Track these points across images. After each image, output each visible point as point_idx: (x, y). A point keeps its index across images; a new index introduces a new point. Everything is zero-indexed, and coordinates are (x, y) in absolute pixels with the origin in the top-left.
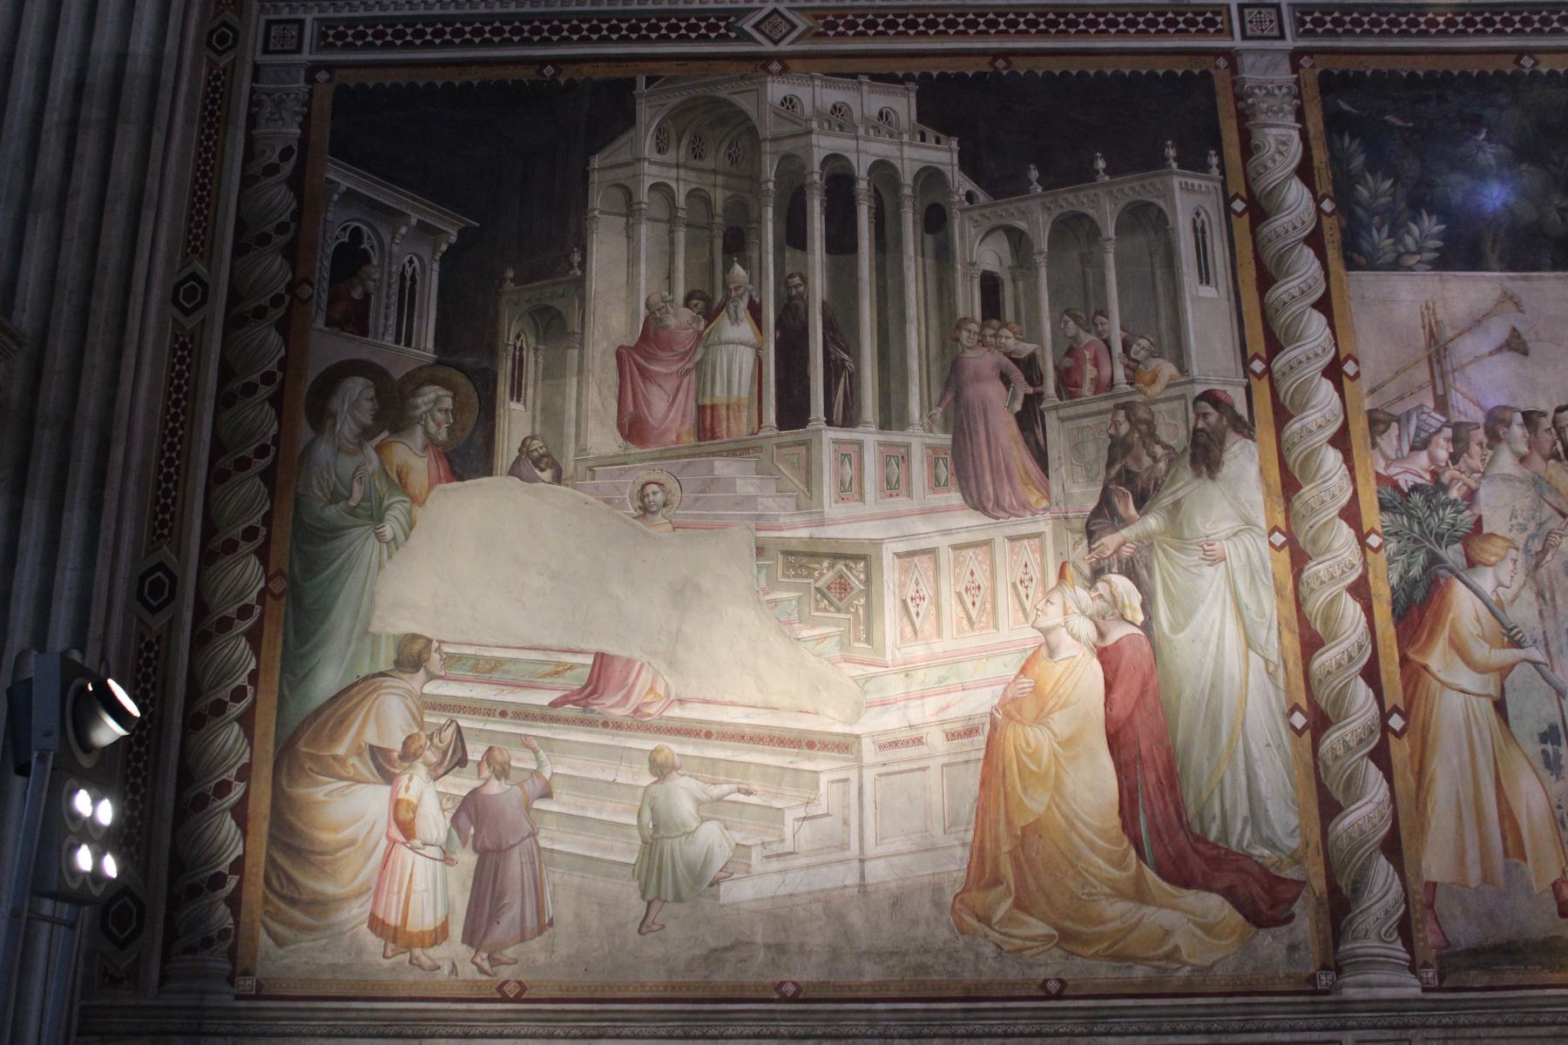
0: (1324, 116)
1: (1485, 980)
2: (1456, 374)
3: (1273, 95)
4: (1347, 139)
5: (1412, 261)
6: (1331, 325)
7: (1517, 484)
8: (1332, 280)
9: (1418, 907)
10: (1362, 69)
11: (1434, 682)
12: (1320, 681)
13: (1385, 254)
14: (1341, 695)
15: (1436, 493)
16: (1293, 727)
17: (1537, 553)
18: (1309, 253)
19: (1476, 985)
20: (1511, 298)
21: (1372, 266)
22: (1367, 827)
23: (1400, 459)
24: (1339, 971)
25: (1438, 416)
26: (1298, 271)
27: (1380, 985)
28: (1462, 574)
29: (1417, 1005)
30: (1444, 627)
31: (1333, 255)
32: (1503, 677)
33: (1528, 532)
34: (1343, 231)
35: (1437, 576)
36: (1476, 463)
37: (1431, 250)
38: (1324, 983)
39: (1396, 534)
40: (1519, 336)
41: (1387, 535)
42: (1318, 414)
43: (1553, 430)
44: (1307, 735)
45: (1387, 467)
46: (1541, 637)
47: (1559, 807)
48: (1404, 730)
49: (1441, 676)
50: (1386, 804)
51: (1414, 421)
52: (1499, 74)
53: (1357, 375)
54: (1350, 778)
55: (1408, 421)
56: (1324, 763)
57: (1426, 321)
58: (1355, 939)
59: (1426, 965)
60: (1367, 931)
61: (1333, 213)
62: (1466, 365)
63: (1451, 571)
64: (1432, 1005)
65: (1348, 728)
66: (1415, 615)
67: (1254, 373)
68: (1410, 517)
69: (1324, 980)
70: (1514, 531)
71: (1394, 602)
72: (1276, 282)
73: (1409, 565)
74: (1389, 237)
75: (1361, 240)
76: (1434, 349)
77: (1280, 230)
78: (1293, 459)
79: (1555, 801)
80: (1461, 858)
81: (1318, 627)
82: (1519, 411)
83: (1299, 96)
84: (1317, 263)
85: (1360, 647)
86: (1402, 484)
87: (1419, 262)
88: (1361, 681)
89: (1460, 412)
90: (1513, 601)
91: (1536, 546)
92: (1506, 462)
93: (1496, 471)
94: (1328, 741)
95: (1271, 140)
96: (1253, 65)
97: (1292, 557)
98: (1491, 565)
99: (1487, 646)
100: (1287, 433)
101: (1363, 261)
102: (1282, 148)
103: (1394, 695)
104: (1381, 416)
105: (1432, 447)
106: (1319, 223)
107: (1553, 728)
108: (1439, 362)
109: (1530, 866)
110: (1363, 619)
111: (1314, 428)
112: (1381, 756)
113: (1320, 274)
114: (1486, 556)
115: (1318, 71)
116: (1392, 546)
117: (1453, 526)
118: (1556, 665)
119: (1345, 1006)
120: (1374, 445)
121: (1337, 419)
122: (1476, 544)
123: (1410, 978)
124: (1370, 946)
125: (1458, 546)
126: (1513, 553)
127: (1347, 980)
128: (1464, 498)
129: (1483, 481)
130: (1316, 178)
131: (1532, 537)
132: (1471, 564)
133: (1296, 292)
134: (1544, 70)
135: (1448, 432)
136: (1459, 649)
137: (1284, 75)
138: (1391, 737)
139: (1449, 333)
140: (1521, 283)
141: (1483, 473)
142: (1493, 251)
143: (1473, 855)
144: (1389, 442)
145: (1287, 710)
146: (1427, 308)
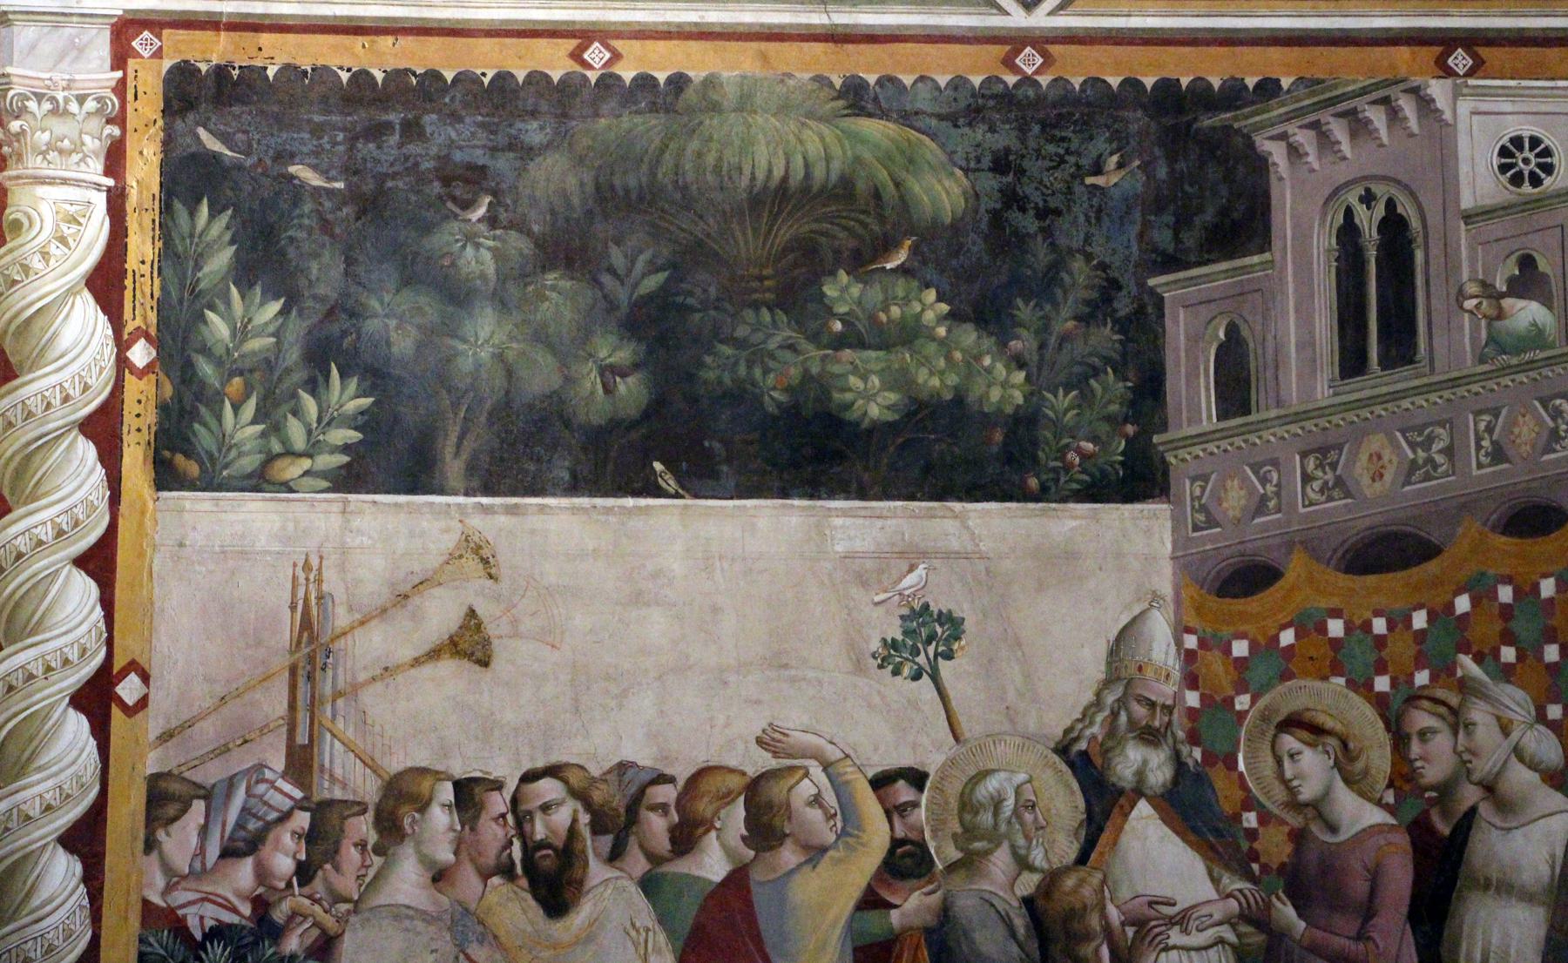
0: (164, 167)
2: (340, 702)
3: (66, 113)
4: (204, 209)
5: (292, 470)
6: (107, 603)
7: (420, 925)
8: (124, 508)
10: (258, 63)
13: (240, 454)
18: (87, 451)
20: (477, 549)
21: (209, 483)
23: (198, 873)
25: (287, 787)
26: (58, 488)
31: (135, 458)
34: (163, 408)
36: (347, 884)
37: (335, 450)
40: (479, 626)
43: (510, 818)
45: (169, 889)
52: (537, 79)
53: (143, 703)
57: (301, 593)
61: (149, 368)
72: (9, 511)
74: (254, 422)
75: (197, 426)
77: (35, 405)
82: (449, 778)
83: (120, 119)
84: (100, 472)
87: (306, 473)
89: (333, 779)
93: (382, 899)
95: (46, 210)
96: (33, 47)
101: (193, 469)
102: (67, 230)
104: (175, 787)
105: (266, 850)
106: (118, 387)
108: (310, 677)
111: (35, 812)
113: (100, 496)
115: (167, 64)
120: (150, 845)
129: (353, 919)
130: (128, 294)
133: (46, 533)
134: (627, 74)
135: (303, 820)
137: (96, 72)
139: (342, 618)
140: (502, 520)
142: (457, 454)
144: (181, 841)
146: (307, 567)
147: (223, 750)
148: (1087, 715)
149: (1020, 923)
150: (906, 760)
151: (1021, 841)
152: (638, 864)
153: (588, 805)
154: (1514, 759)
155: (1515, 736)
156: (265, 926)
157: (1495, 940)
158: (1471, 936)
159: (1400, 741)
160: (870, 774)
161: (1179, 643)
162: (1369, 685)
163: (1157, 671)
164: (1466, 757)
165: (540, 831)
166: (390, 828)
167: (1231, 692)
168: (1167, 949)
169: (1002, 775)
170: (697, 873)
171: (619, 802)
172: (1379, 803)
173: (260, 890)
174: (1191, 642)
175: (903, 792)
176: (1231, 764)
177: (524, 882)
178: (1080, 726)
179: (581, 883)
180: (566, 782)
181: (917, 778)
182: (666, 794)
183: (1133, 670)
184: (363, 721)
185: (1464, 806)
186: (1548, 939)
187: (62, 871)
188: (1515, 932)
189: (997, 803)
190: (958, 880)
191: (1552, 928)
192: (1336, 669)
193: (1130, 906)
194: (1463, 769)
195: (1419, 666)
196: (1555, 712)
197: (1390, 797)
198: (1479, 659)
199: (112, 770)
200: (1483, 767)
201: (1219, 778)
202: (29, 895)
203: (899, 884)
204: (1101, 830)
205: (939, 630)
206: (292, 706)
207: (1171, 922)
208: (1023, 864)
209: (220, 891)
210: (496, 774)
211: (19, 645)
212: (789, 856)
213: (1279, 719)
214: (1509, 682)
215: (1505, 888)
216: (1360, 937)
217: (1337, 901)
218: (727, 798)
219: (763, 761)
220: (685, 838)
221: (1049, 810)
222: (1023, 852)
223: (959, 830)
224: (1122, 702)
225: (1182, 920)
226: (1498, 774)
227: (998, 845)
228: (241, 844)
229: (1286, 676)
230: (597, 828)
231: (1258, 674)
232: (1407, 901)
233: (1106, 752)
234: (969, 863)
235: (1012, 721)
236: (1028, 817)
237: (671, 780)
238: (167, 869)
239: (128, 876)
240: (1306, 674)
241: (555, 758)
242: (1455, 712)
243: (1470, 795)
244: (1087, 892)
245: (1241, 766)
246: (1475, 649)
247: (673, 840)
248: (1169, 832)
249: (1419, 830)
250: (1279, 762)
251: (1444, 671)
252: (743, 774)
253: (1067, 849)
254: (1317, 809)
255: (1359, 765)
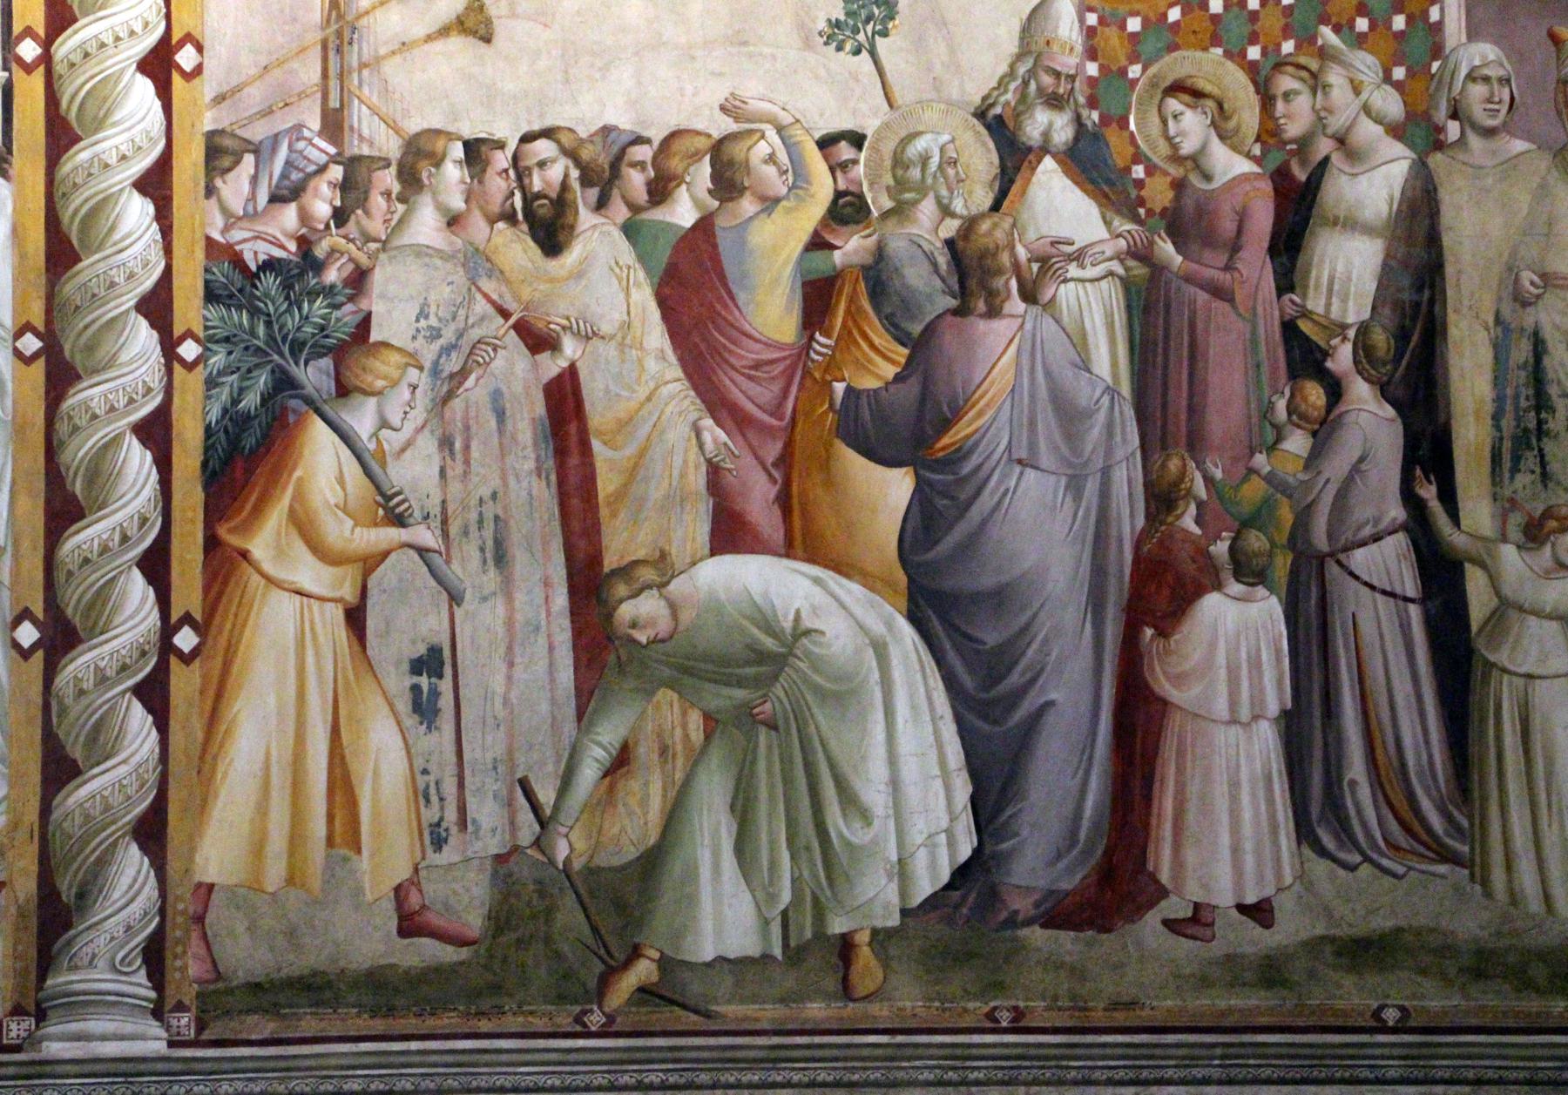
1: (269, 1028)
2: (365, 72)
7: (438, 262)
9: (180, 920)
11: (256, 578)
12: (70, 573)
14: (102, 601)
15: (301, 274)
16: (16, 645)
17: (452, 376)
19: (253, 1037)
22: (116, 799)
23: (251, 216)
24: (41, 1016)
25: (323, 144)
27: (104, 1038)
28: (326, 408)
29: (160, 1066)
30: (284, 488)
32: (367, 574)
33: (442, 341)
35: (284, 409)
36: (376, 227)
38: (13, 1034)
39: (227, 340)
41: (207, 343)
42: (126, 136)
43: (512, 173)
44: (40, 654)
45: (226, 229)
46: (436, 510)
47: (425, 772)
48: (196, 652)
49: (267, 567)
50: (151, 765)
51: (283, 153)
53: (198, 70)
54: (98, 727)
55: (274, 150)
56: (60, 703)
58: (74, 968)
59: (180, 1007)
60: (94, 956)
62: (384, 58)
63: (309, 401)
64: (178, 1067)
65: (107, 648)
66: (238, 473)
67: (20, 61)
68: (254, 312)
69: (16, 1029)
70: (420, 340)
71: (208, 449)
73: (241, 390)
76: (334, 27)
78: (73, 210)
79: (419, 763)
80: (258, 849)
81: (78, 488)
82: (459, 139)
85: (143, 521)
86: (248, 257)
88: (137, 574)
90: (403, 450)
91: (453, 364)
92: (426, 226)
93: (406, 239)
94: (71, 667)
97: (49, 376)
98: (372, 394)
99: (349, 523)
100: (64, 168)
103: (188, 593)
104: (227, 142)
105: (307, 198)
107: (435, 651)
108: (339, 50)
109: (364, 863)
110: (155, 476)
111: (113, 160)
112: (154, 694)
114: (369, 379)
116: (218, 359)
117: (323, 328)
118: (455, 552)
119: (45, 1069)
120: (210, 191)
121: (156, 143)
122: (356, 358)
123: (155, 1028)
124: (99, 979)
125: (326, 363)
126: (413, 374)
127: (51, 1030)
128: (348, 282)
129: (383, 256)
131: (448, 350)
132: (343, 391)
135: (337, 172)
136: (303, 526)
138: (173, 660)
141: (385, 242)
143: (277, 842)
144: (236, 187)
145: (9, 619)
147: (268, 112)
148: (1002, 84)
149: (943, 260)
150: (846, 124)
151: (944, 192)
152: (620, 212)
153: (578, 162)
154: (1363, 117)
155: (1364, 96)
156: (309, 261)
157: (1340, 268)
158: (1322, 261)
159: (1267, 101)
160: (817, 135)
161: (1082, 20)
162: (1243, 54)
163: (1063, 46)
164: (1323, 114)
165: (537, 184)
166: (411, 181)
167: (1123, 61)
168: (1065, 281)
169: (929, 137)
170: (668, 219)
171: (604, 161)
172: (1248, 156)
173: (304, 231)
174: (1092, 19)
175: (845, 151)
176: (1123, 122)
177: (525, 227)
178: (995, 93)
179: (572, 227)
180: (558, 142)
181: (857, 140)
182: (643, 153)
183: (1042, 41)
184: (386, 91)
185: (1320, 157)
186: (1385, 265)
187: (137, 212)
188: (1357, 261)
189: (925, 160)
190: (891, 224)
191: (1388, 255)
192: (1216, 41)
193: (1034, 246)
194: (1320, 121)
195: (1286, 38)
196: (1399, 73)
197: (1257, 150)
198: (1337, 29)
199: (175, 127)
200: (1336, 123)
201: (1113, 137)
202: (112, 229)
203: (844, 229)
204: (1012, 182)
205: (876, 11)
206: (325, 75)
207: (1070, 258)
208: (946, 211)
209: (270, 231)
210: (499, 135)
211: (91, 18)
212: (748, 205)
213: (1167, 83)
214: (1360, 48)
215: (1350, 224)
216: (1228, 268)
217: (1209, 240)
218: (695, 156)
219: (723, 125)
220: (660, 191)
221: (968, 166)
222: (945, 201)
223: (891, 182)
224: (1032, 72)
225: (1078, 257)
226: (1349, 129)
227: (925, 196)
228: (285, 192)
229: (1173, 47)
230: (586, 181)
231: (1147, 48)
232: (1268, 238)
233: (1017, 115)
234: (900, 211)
235: (937, 90)
236: (951, 172)
237: (648, 141)
238: (225, 211)
239: (192, 217)
240: (1188, 46)
241: (549, 122)
242: (1314, 76)
243: (1324, 146)
244: (999, 235)
245: (1132, 126)
246: (1334, 20)
247: (650, 192)
248: (1069, 182)
249: (1281, 176)
250: (1164, 122)
251: (1307, 41)
252: (709, 136)
253: (983, 198)
254: (1196, 161)
255: (1232, 124)
